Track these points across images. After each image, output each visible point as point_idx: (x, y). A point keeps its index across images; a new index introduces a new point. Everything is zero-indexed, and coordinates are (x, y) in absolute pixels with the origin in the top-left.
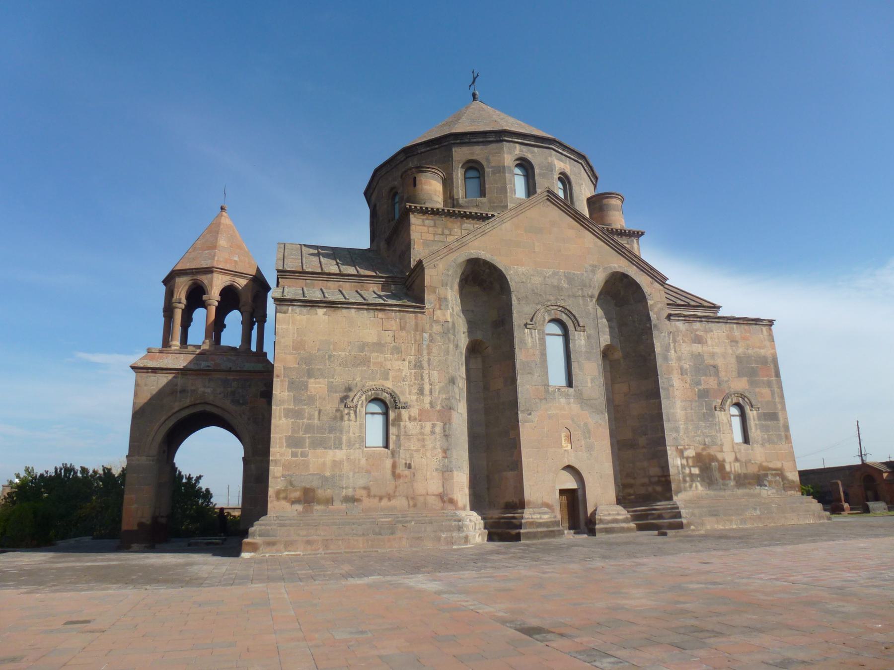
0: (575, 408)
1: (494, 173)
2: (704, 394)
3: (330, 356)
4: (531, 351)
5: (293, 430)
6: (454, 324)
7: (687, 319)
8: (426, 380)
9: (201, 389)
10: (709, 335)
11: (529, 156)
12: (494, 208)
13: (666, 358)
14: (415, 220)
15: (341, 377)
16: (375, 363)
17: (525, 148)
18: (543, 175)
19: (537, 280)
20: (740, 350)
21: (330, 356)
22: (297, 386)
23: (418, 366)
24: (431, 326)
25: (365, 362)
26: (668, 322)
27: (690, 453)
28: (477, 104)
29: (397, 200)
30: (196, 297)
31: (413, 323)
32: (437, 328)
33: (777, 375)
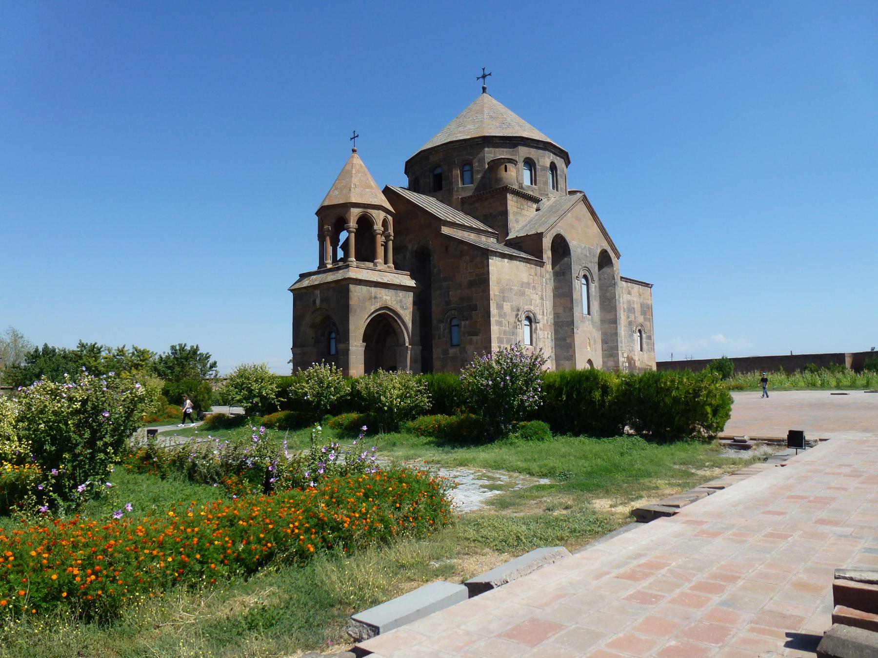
0: (591, 326)
2: (630, 323)
11: (556, 162)
12: (541, 194)
14: (509, 196)
15: (517, 301)
19: (579, 250)
23: (542, 299)
27: (625, 355)
29: (467, 168)
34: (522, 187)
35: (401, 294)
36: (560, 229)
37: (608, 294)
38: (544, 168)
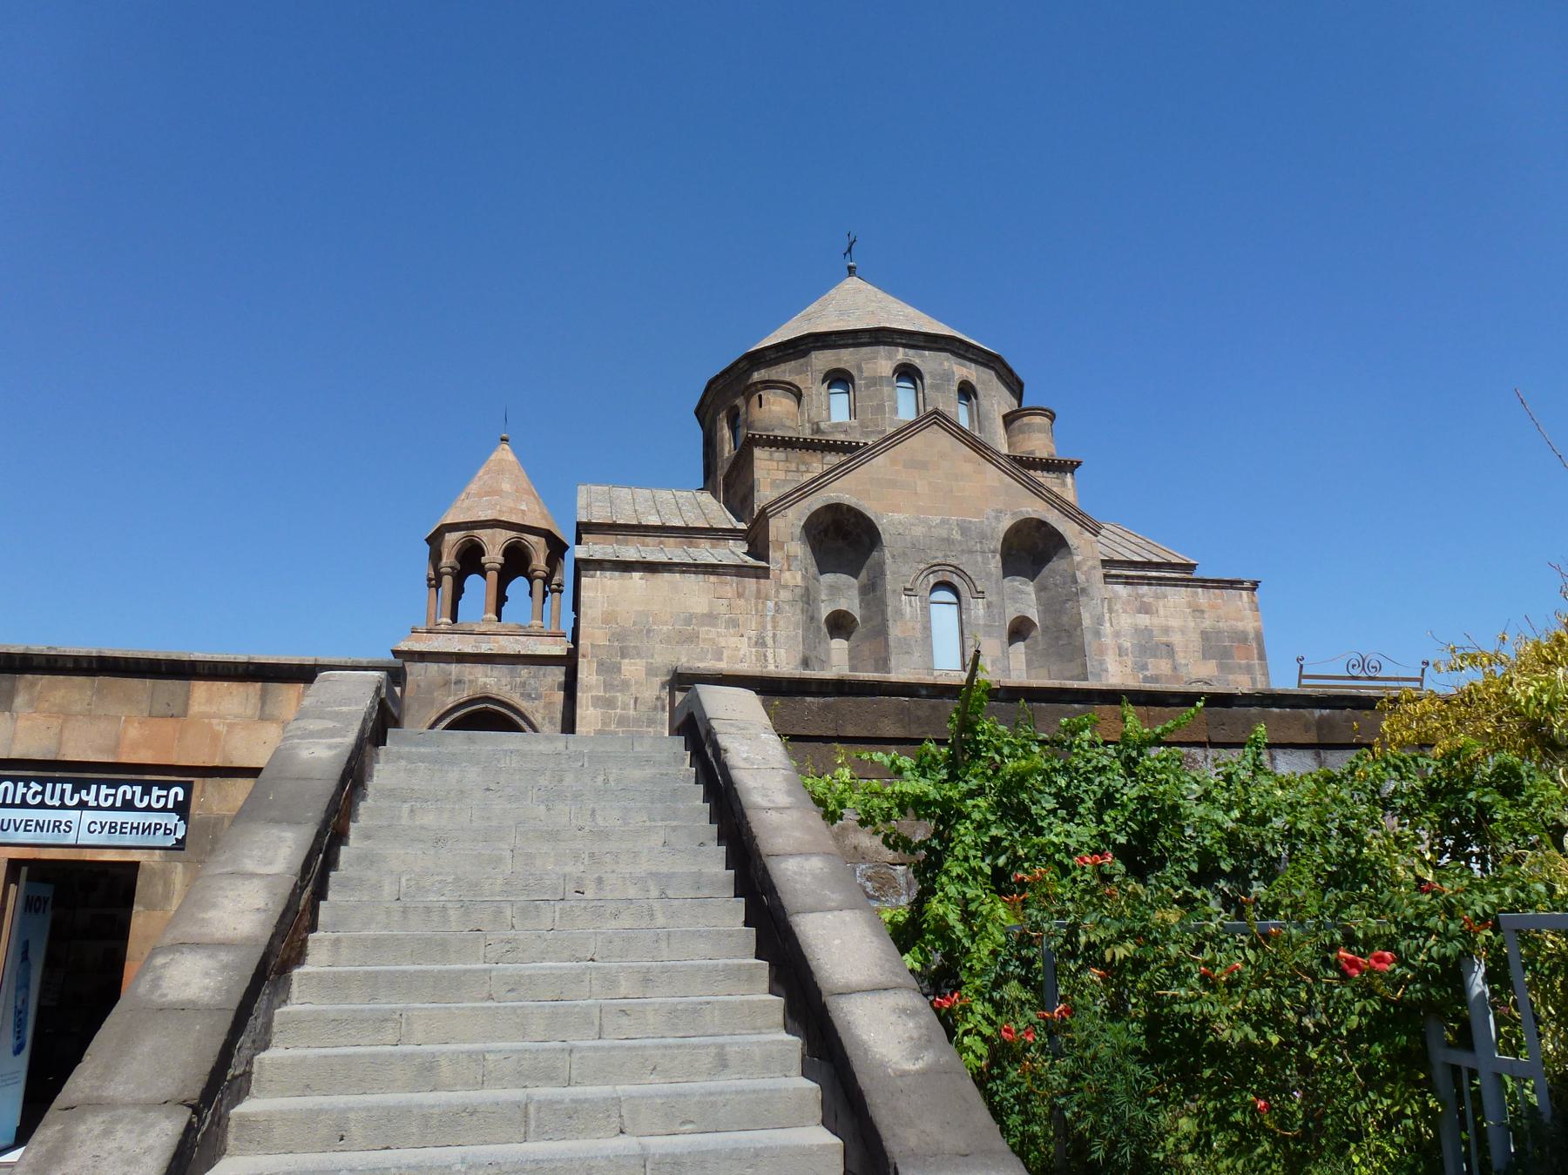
1: (868, 386)
3: (649, 631)
4: (910, 624)
5: (604, 724)
6: (807, 589)
7: (1128, 582)
8: (771, 660)
9: (482, 680)
10: (1161, 603)
11: (917, 362)
12: (867, 434)
13: (1098, 634)
16: (704, 640)
17: (911, 352)
18: (935, 387)
19: (918, 531)
20: (1207, 624)
21: (649, 631)
22: (608, 669)
23: (760, 643)
24: (777, 592)
25: (692, 638)
26: (1102, 585)
28: (853, 283)
30: (471, 558)
31: (754, 587)
32: (785, 595)
33: (1262, 657)
34: (818, 430)
35: (524, 671)
36: (842, 491)
37: (1065, 619)
38: (875, 381)
